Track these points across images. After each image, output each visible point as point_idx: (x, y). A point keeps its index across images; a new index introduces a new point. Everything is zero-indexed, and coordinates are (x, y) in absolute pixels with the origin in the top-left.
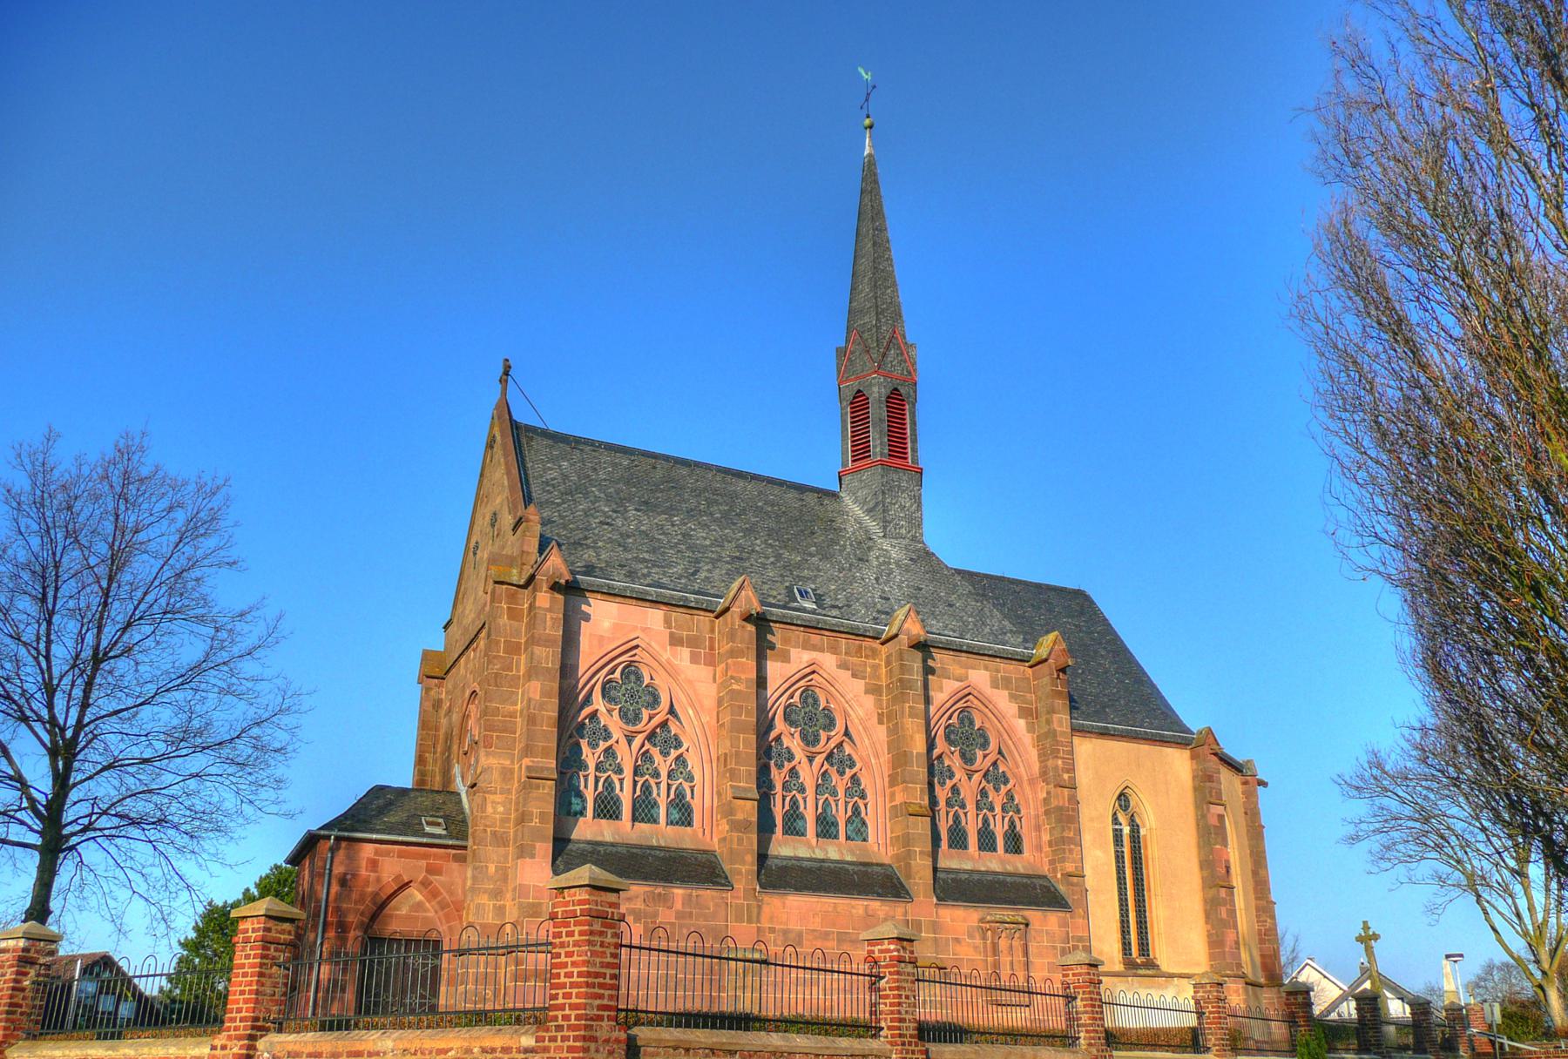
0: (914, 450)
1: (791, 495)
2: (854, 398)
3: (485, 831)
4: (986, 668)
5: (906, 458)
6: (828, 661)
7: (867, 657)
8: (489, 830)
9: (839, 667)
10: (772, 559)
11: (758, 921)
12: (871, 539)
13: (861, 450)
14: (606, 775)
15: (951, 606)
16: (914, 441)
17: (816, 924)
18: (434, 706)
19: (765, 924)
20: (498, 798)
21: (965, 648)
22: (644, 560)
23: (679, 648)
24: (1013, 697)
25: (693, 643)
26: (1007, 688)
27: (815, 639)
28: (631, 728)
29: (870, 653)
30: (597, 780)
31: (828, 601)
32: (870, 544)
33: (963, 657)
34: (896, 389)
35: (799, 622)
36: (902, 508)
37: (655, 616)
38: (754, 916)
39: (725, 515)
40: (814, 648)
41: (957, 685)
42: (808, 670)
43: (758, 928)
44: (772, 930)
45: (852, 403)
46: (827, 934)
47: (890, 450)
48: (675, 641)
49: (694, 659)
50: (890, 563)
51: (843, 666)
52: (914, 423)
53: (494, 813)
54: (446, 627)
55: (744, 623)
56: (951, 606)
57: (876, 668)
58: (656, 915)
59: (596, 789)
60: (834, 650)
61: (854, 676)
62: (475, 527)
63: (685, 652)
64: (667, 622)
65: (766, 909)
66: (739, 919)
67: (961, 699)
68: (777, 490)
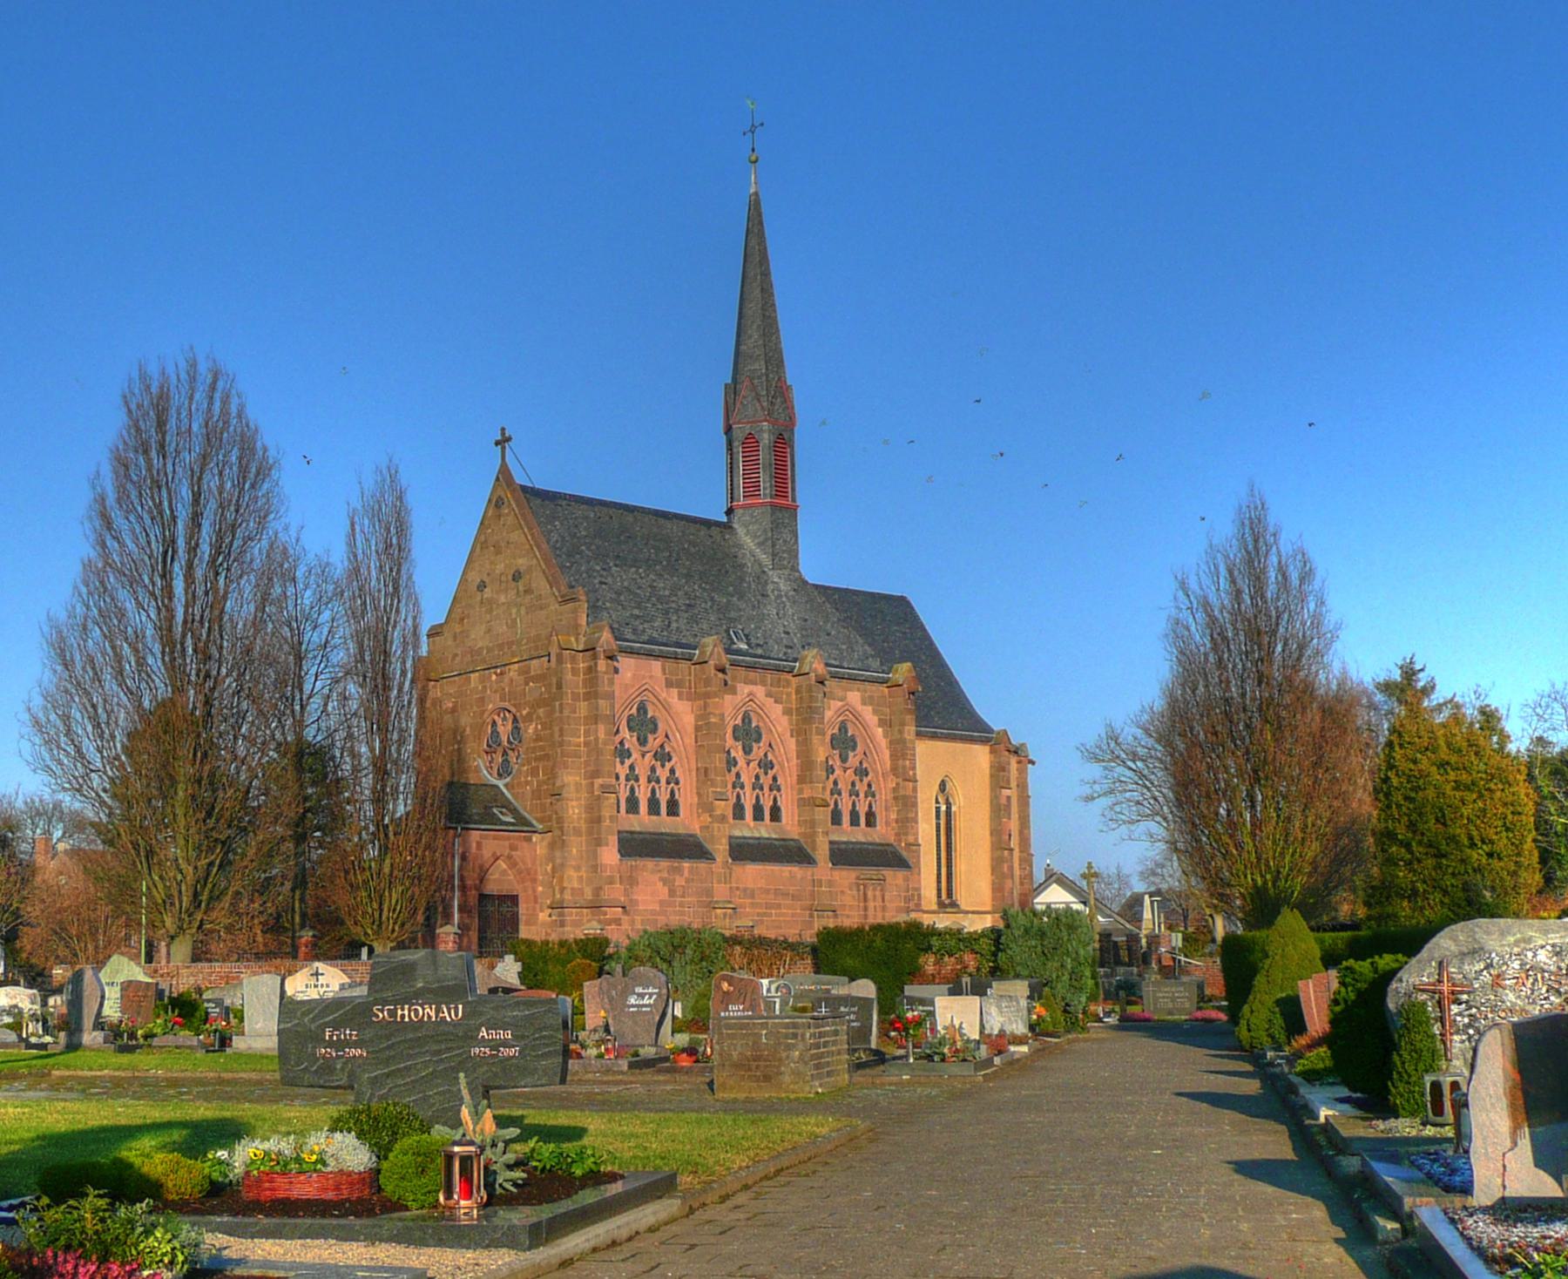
0: (793, 490)
6: (760, 691)
16: (793, 481)
17: (762, 884)
27: (752, 675)
37: (656, 665)
38: (727, 879)
44: (738, 888)
49: (680, 697)
51: (769, 695)
52: (793, 465)
57: (789, 694)
60: (763, 683)
61: (776, 702)
63: (675, 691)
64: (664, 670)
66: (719, 882)
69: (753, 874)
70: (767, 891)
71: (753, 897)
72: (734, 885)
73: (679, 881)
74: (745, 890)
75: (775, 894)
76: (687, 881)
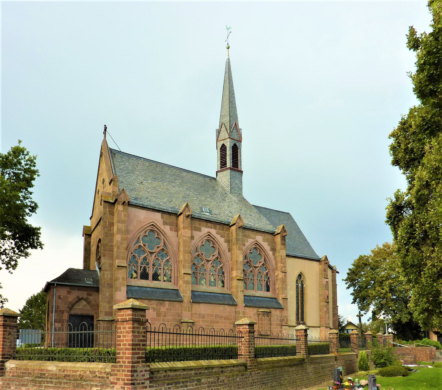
1: (201, 178)
2: (222, 146)
3: (105, 283)
4: (261, 236)
5: (238, 168)
6: (213, 232)
7: (225, 231)
8: (106, 282)
9: (216, 233)
10: (195, 198)
11: (192, 311)
12: (226, 193)
13: (223, 164)
14: (144, 266)
15: (251, 215)
18: (88, 244)
19: (193, 312)
20: (108, 273)
21: (255, 229)
22: (154, 197)
23: (166, 226)
24: (269, 245)
25: (170, 224)
26: (267, 242)
27: (209, 224)
28: (151, 251)
29: (226, 230)
30: (141, 267)
31: (213, 212)
32: (226, 195)
33: (255, 232)
34: (235, 144)
35: (204, 219)
36: (236, 184)
38: (190, 310)
39: (180, 184)
40: (209, 227)
41: (252, 240)
42: (207, 234)
43: (191, 313)
44: (196, 314)
45: (221, 148)
46: (212, 315)
47: (233, 165)
48: (165, 223)
49: (171, 230)
50: (232, 202)
51: (218, 233)
53: (107, 277)
54: (91, 218)
55: (187, 218)
56: (251, 215)
58: (160, 309)
59: (140, 270)
61: (221, 236)
62: (98, 184)
63: (168, 227)
65: (194, 307)
66: (185, 311)
67: (253, 245)
68: (196, 176)
69: (202, 309)
70: (212, 315)
71: (204, 317)
72: (193, 312)
73: (163, 309)
74: (200, 314)
75: (216, 317)
76: (167, 309)
